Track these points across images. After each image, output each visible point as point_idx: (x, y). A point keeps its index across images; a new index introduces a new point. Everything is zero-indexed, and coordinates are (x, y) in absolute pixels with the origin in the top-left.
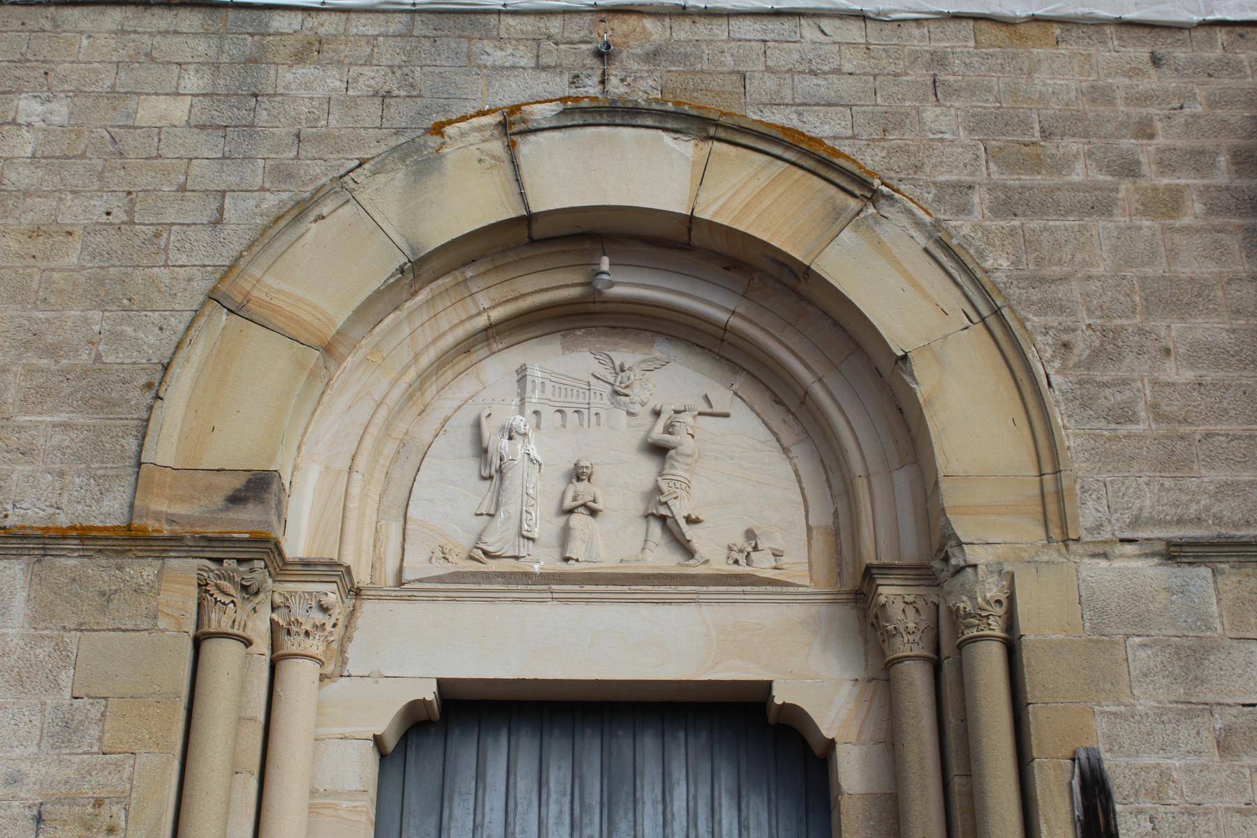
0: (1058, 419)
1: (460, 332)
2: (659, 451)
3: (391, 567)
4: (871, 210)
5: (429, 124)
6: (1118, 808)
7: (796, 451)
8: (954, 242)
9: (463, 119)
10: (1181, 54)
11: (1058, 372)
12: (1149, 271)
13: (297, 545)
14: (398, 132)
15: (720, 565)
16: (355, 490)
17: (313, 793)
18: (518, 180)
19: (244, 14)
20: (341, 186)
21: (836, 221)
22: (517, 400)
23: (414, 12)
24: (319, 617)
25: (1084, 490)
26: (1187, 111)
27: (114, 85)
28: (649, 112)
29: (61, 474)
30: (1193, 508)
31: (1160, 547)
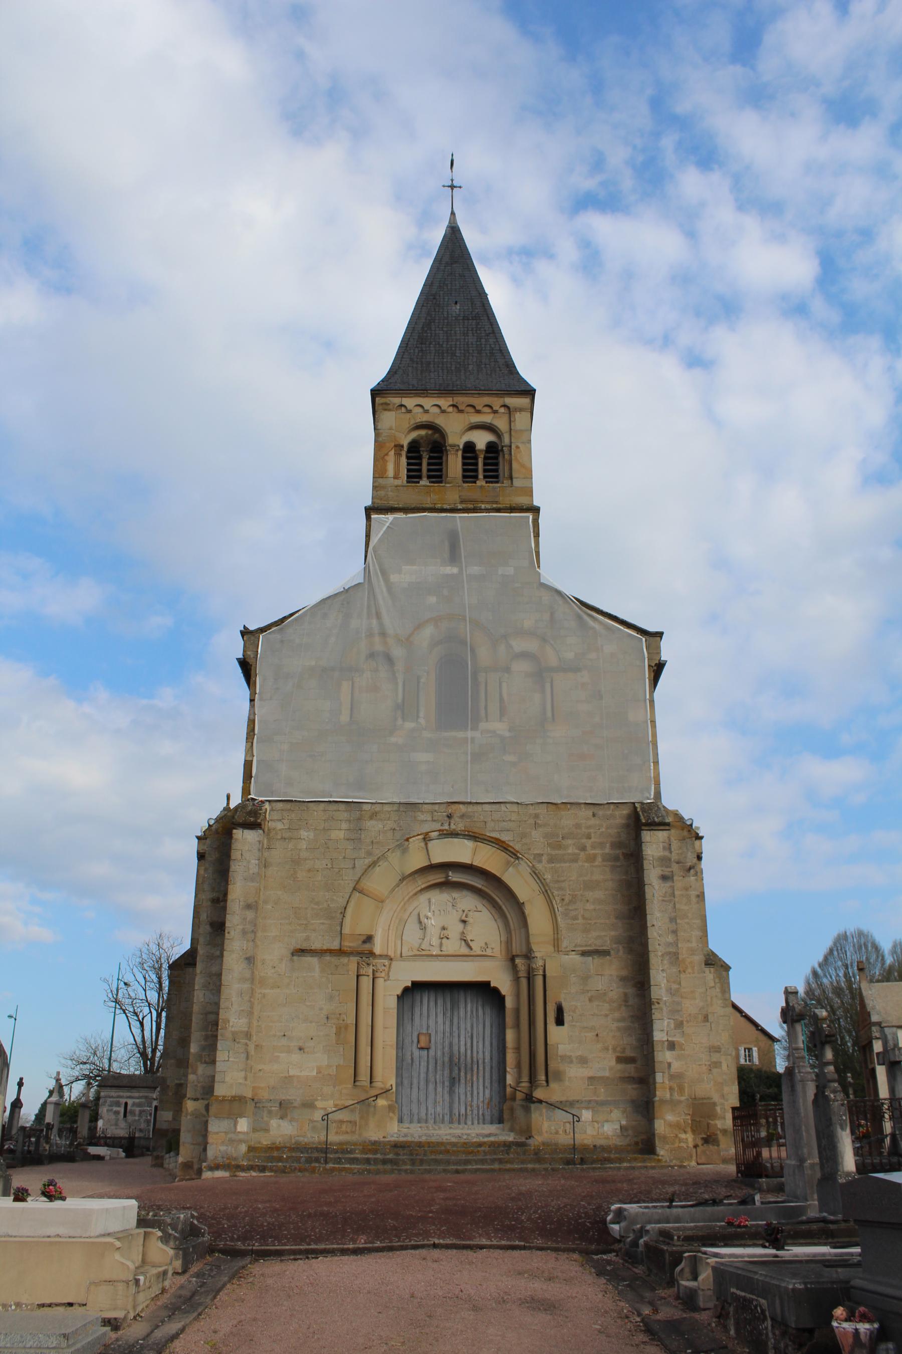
0: (559, 919)
1: (414, 891)
2: (464, 922)
3: (399, 953)
4: (517, 861)
5: (405, 838)
6: (565, 1014)
7: (499, 920)
8: (537, 872)
9: (414, 836)
10: (601, 813)
11: (561, 907)
12: (585, 878)
13: (377, 950)
14: (397, 841)
15: (480, 953)
16: (390, 935)
17: (384, 1008)
18: (428, 854)
19: (355, 804)
20: (383, 857)
21: (508, 864)
22: (428, 908)
23: (400, 803)
24: (383, 968)
25: (564, 938)
26: (601, 830)
27: (324, 827)
28: (461, 835)
29: (323, 936)
30: (590, 942)
31: (580, 952)
